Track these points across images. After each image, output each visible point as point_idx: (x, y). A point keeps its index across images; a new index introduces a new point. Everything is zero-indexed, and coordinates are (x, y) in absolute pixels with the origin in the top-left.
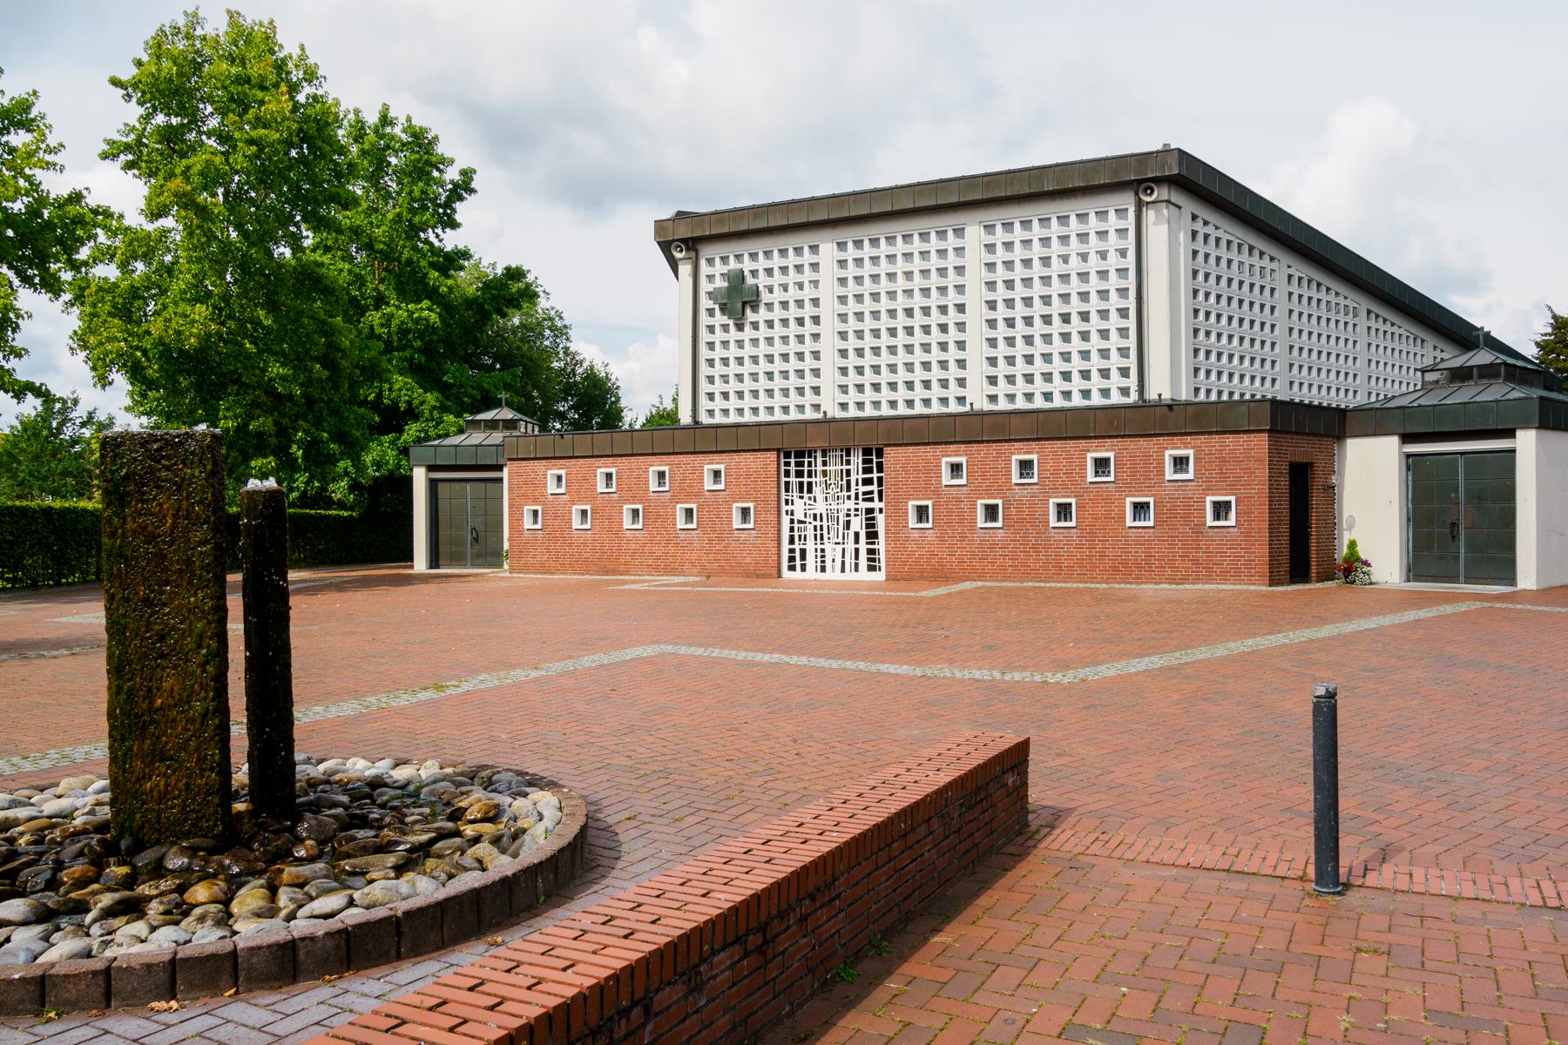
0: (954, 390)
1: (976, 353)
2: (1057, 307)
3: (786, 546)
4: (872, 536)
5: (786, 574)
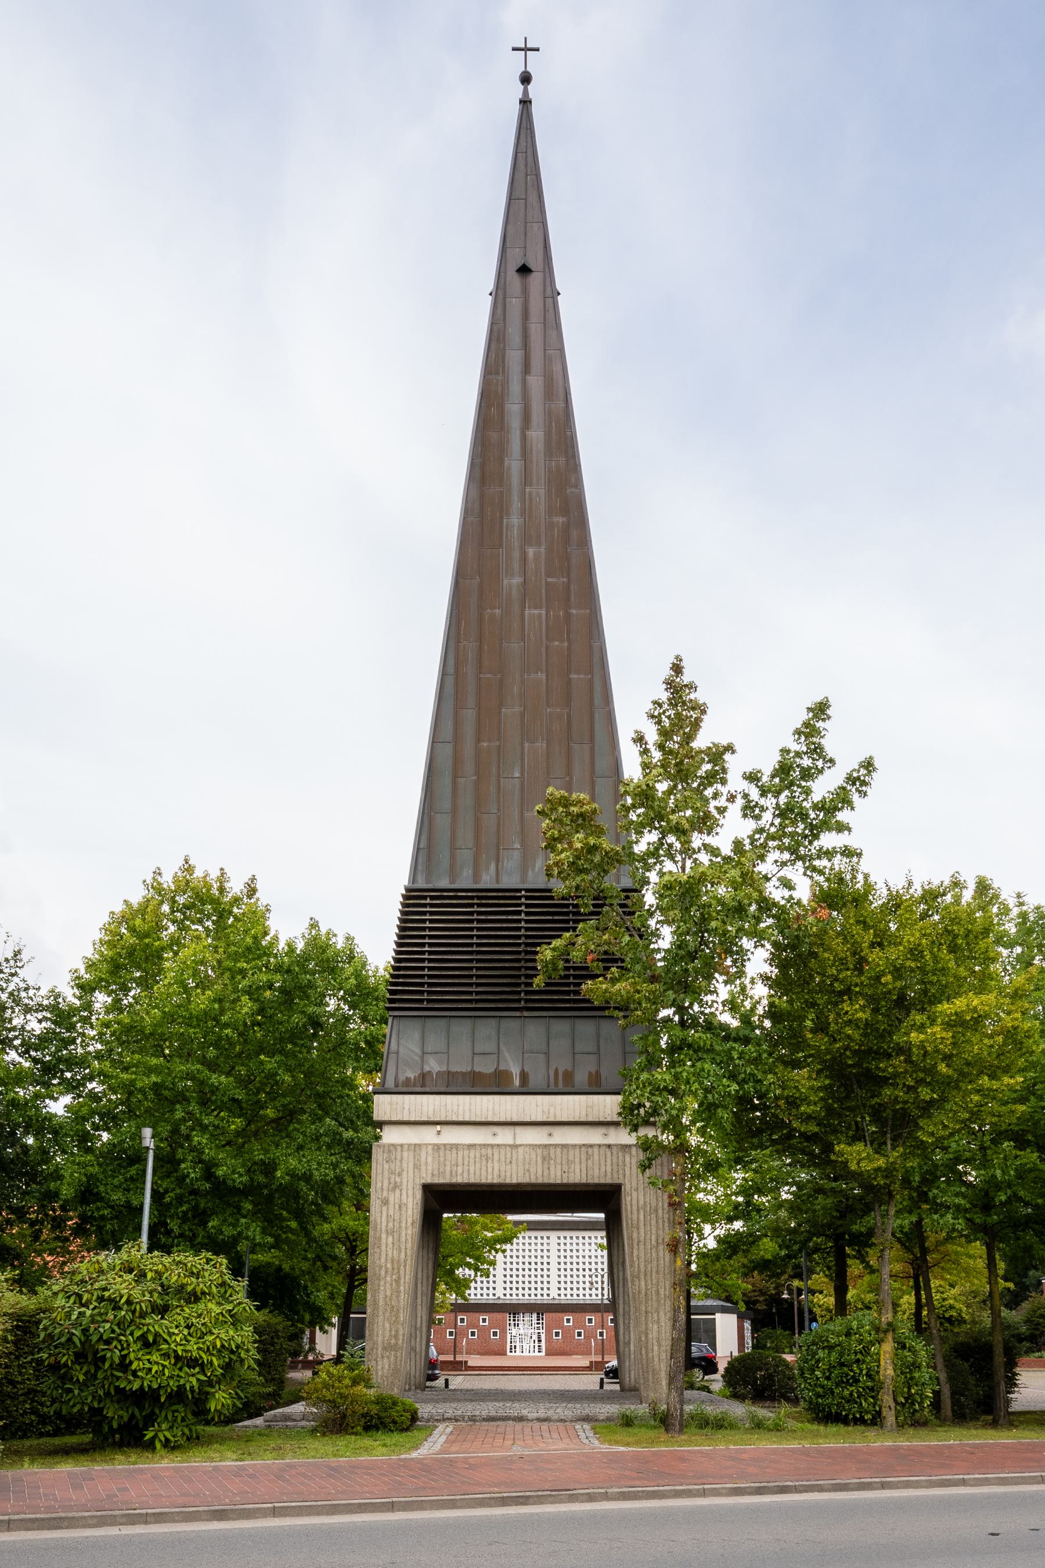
0: (491, 1291)
1: (554, 1279)
2: (581, 1266)
3: (509, 1344)
4: (540, 1341)
5: (508, 1353)
